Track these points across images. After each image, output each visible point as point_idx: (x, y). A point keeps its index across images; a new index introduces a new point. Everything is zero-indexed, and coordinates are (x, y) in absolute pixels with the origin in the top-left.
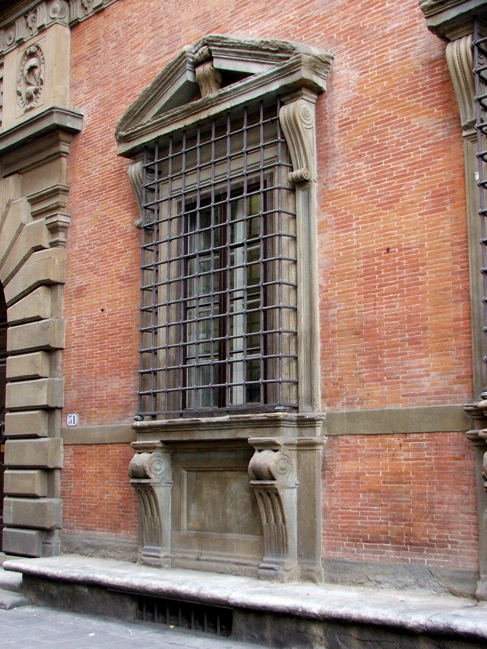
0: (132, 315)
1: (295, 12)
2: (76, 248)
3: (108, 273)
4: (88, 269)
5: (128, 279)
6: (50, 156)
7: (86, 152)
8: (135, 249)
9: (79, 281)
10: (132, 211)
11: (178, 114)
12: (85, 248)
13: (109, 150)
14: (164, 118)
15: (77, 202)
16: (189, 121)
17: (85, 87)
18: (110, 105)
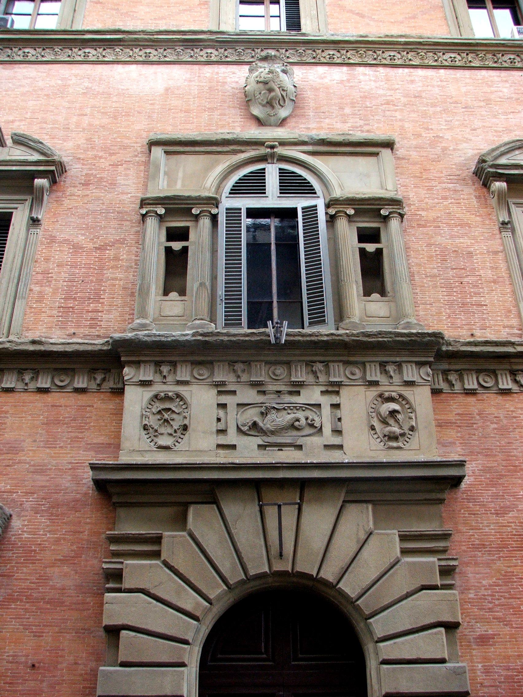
2: (471, 596)
4: (494, 618)
7: (471, 508)
9: (480, 629)
12: (487, 597)
13: (507, 514)
15: (465, 551)
17: (459, 449)
18: (500, 475)
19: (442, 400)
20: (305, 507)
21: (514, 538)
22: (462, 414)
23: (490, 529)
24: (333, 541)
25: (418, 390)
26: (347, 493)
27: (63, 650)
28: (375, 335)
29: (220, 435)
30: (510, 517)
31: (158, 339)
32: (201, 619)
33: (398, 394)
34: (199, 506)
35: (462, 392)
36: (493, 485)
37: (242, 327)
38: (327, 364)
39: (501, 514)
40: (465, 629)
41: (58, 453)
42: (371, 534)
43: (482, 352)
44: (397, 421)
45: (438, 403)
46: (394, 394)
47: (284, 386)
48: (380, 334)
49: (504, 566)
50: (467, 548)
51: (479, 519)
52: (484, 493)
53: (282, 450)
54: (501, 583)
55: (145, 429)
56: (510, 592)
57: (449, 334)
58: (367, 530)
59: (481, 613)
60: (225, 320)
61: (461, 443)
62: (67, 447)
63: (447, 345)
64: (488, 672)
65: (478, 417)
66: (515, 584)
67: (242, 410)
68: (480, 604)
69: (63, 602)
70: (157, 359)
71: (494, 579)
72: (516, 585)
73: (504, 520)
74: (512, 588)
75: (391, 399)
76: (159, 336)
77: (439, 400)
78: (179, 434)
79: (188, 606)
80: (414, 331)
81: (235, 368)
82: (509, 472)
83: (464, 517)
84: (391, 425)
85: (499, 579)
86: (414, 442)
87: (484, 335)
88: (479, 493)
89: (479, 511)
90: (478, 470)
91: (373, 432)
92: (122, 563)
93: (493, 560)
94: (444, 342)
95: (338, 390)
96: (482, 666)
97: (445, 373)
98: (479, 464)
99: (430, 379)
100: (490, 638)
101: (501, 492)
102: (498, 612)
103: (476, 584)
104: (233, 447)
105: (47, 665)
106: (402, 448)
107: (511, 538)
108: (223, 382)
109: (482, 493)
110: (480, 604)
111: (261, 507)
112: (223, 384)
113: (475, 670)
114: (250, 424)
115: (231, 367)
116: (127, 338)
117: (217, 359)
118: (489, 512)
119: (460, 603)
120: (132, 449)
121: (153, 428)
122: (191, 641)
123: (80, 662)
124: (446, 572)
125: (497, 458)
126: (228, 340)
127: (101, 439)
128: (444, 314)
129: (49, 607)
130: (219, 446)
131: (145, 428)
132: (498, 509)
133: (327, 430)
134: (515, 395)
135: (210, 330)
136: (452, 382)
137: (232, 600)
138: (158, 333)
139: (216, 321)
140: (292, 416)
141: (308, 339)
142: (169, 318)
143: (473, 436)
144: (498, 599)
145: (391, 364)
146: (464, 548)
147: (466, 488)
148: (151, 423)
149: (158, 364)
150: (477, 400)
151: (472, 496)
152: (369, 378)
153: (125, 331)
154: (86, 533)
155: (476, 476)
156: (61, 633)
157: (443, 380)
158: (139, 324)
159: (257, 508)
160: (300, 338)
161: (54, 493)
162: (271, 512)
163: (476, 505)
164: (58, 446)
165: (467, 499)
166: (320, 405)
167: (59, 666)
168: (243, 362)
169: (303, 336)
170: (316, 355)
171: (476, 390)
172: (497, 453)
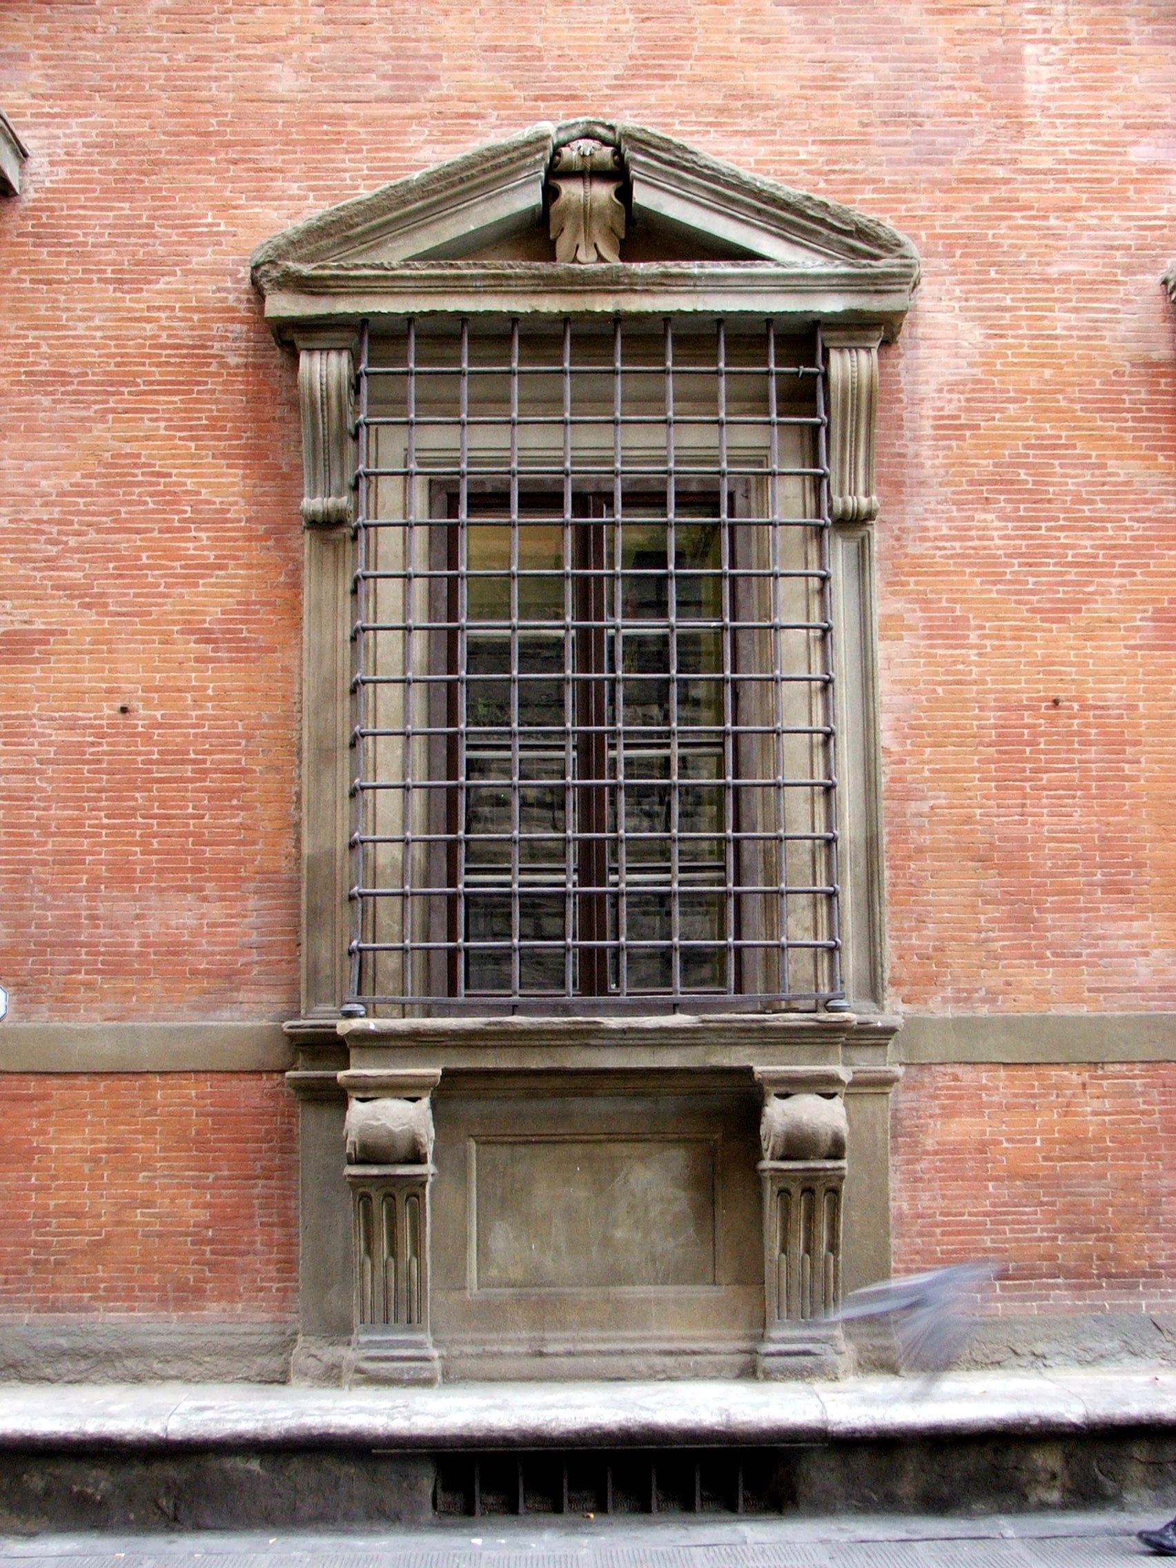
0: (249, 738)
1: (814, 148)
4: (54, 587)
5: (230, 641)
7: (43, 262)
8: (261, 566)
10: (246, 467)
11: (518, 277)
12: (44, 527)
13: (150, 282)
14: (465, 272)
16: (551, 305)
17: (34, 77)
18: (154, 163)
21: (160, 356)
23: (89, 328)
30: (159, 292)
36: (125, 194)
39: (132, 281)
49: (113, 438)
50: (13, 383)
52: (90, 218)
54: (94, 488)
56: (119, 512)
59: (22, 572)
61: (44, 58)
66: (137, 490)
68: (22, 546)
71: (78, 474)
72: (140, 495)
74: (122, 503)
82: (181, 152)
83: (18, 290)
85: (91, 476)
88: (75, 217)
89: (65, 271)
90: (85, 145)
93: (83, 419)
98: (94, 125)
100: (35, 642)
101: (145, 214)
102: (68, 569)
103: (20, 489)
107: (149, 356)
109: (84, 217)
110: (22, 546)
118: (95, 277)
125: (155, 109)
143: (90, 35)
144: (78, 534)
151: (53, 226)
155: (78, 163)
163: (58, 254)
165: (37, 235)
172: (154, 92)
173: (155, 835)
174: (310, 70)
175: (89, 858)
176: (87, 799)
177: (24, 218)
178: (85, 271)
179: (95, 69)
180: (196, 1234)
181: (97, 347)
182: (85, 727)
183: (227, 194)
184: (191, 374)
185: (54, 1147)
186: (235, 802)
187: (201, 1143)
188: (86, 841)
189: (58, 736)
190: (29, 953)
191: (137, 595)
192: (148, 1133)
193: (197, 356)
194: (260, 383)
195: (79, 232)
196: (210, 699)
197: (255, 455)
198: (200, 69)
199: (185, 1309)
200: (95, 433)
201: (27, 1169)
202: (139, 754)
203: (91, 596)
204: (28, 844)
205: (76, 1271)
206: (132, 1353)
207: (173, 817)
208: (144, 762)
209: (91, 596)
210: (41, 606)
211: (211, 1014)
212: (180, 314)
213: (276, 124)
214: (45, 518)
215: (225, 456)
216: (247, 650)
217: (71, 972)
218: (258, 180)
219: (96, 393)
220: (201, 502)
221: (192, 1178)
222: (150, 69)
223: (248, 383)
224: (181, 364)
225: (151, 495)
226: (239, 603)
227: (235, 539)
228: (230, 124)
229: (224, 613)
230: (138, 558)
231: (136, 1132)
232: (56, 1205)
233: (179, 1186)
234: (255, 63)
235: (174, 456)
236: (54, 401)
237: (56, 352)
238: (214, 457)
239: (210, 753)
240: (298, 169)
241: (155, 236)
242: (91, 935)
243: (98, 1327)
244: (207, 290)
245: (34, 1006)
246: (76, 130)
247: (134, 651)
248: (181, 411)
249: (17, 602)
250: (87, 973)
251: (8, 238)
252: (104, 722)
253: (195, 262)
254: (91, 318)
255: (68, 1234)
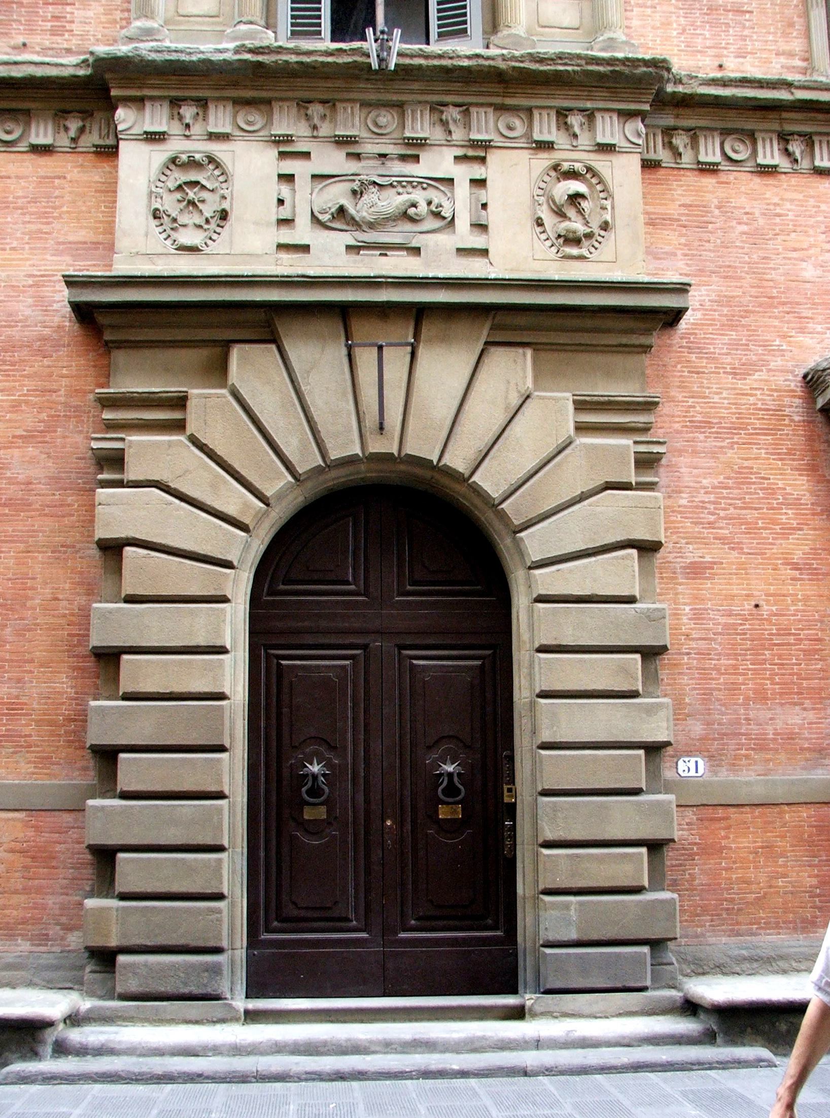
0: (822, 622)
2: (684, 502)
3: (765, 554)
4: (715, 538)
5: (809, 569)
6: (626, 346)
7: (694, 362)
8: (821, 529)
9: (693, 553)
10: (808, 475)
12: (707, 505)
13: (750, 375)
15: (677, 432)
17: (681, 264)
18: (746, 311)
19: (658, 179)
20: (421, 351)
22: (691, 206)
23: (720, 398)
24: (467, 407)
25: (618, 160)
26: (491, 329)
27: (34, 579)
28: (552, 60)
29: (282, 228)
30: (756, 380)
31: (174, 56)
32: (251, 528)
33: (586, 167)
34: (247, 347)
35: (695, 167)
36: (732, 327)
37: (322, 39)
38: (467, 110)
40: (670, 553)
41: (9, 260)
42: (528, 397)
43: (734, 98)
44: (581, 212)
45: (650, 183)
46: (578, 166)
47: (392, 146)
48: (560, 58)
49: (739, 458)
50: (683, 427)
51: (705, 381)
53: (386, 255)
54: (731, 485)
55: (155, 217)
57: (680, 64)
58: (523, 391)
59: (697, 530)
60: (293, 25)
61: (686, 255)
62: (23, 249)
63: (675, 83)
64: (698, 619)
65: (717, 212)
66: (753, 486)
67: (321, 186)
68: (696, 516)
69: (30, 505)
70: (173, 93)
71: (722, 477)
72: (755, 489)
73: (745, 384)
74: (747, 493)
75: (572, 175)
76: (176, 51)
77: (654, 179)
78: (213, 226)
79: (231, 510)
80: (620, 55)
81: (309, 112)
83: (681, 376)
84: (570, 219)
85: (728, 478)
86: (607, 248)
87: (742, 68)
88: (708, 339)
90: (709, 300)
91: (539, 229)
92: (123, 440)
93: (722, 447)
94: (671, 76)
95: (483, 154)
96: (691, 610)
97: (668, 132)
98: (714, 291)
99: (640, 142)
100: (706, 568)
101: (744, 339)
103: (692, 484)
104: (305, 248)
105: (9, 602)
106: (586, 258)
107: (753, 414)
108: (288, 136)
109: (713, 339)
110: (696, 516)
111: (350, 348)
112: (288, 139)
113: (678, 614)
114: (333, 210)
115: (302, 112)
116: (120, 54)
117: (276, 95)
118: (721, 371)
119: (665, 512)
120: (134, 251)
121: (169, 216)
122: (235, 563)
123: (61, 597)
124: (646, 462)
125: (745, 283)
126: (297, 62)
127: (82, 235)
128: (675, 26)
129: (7, 511)
130: (281, 247)
131: (156, 215)
132: (737, 366)
133: (463, 223)
134: (783, 176)
135: (265, 43)
136: (677, 149)
137: (301, 499)
138: (173, 46)
139: (276, 27)
140: (405, 197)
141: (436, 62)
142: (192, 19)
143: (707, 244)
145: (576, 112)
146: (677, 426)
147: (688, 329)
148: (166, 207)
149: (175, 103)
150: (718, 183)
151: (697, 343)
152: (536, 137)
153: (115, 41)
154: (62, 392)
156: (29, 552)
157: (664, 145)
158: (139, 28)
159: (344, 351)
160: (422, 62)
161: (5, 326)
162: (366, 358)
163: (702, 358)
164: (8, 247)
165: (689, 348)
166: (453, 180)
167: (29, 604)
168: (323, 102)
169: (427, 57)
170: (448, 92)
171: (717, 164)
172: (743, 274)
173: (777, 674)
174: (822, 266)
175: (743, 687)
176: (740, 655)
177: (681, 338)
178: (716, 368)
179: (712, 261)
180: (811, 892)
181: (726, 408)
182: (736, 615)
183: (785, 329)
184: (775, 425)
185: (733, 846)
186: (817, 657)
187: (811, 843)
188: (740, 678)
189: (723, 620)
190: (714, 739)
191: (758, 544)
192: (783, 837)
193: (778, 415)
194: (812, 431)
195: (711, 347)
196: (800, 601)
197: (813, 469)
198: (765, 264)
199: (807, 933)
200: (729, 455)
201: (721, 858)
202: (766, 630)
203: (734, 543)
204: (710, 679)
205: (749, 914)
206: (781, 958)
207: (786, 664)
208: (768, 634)
209: (734, 543)
210: (709, 549)
211: (812, 772)
212: (767, 393)
213: (806, 294)
214: (707, 500)
215: (797, 470)
216: (817, 574)
217: (738, 749)
218: (800, 323)
219: (728, 433)
220: (787, 494)
221: (807, 861)
222: (740, 263)
223: (805, 431)
224: (770, 419)
225: (761, 489)
226: (811, 549)
227: (807, 515)
228: (784, 292)
229: (804, 554)
230: (757, 523)
231: (776, 837)
232: (737, 878)
233: (800, 866)
234: (793, 261)
235: (771, 469)
236: (706, 437)
237: (704, 410)
238: (792, 470)
239: (802, 630)
240: (820, 318)
241: (750, 350)
242: (747, 729)
243: (761, 944)
244: (780, 380)
245: (718, 768)
246: (705, 293)
247: (759, 574)
248: (773, 444)
249: (695, 546)
250: (746, 750)
251: (674, 348)
252: (746, 613)
253: (772, 365)
254: (721, 393)
255: (745, 893)
